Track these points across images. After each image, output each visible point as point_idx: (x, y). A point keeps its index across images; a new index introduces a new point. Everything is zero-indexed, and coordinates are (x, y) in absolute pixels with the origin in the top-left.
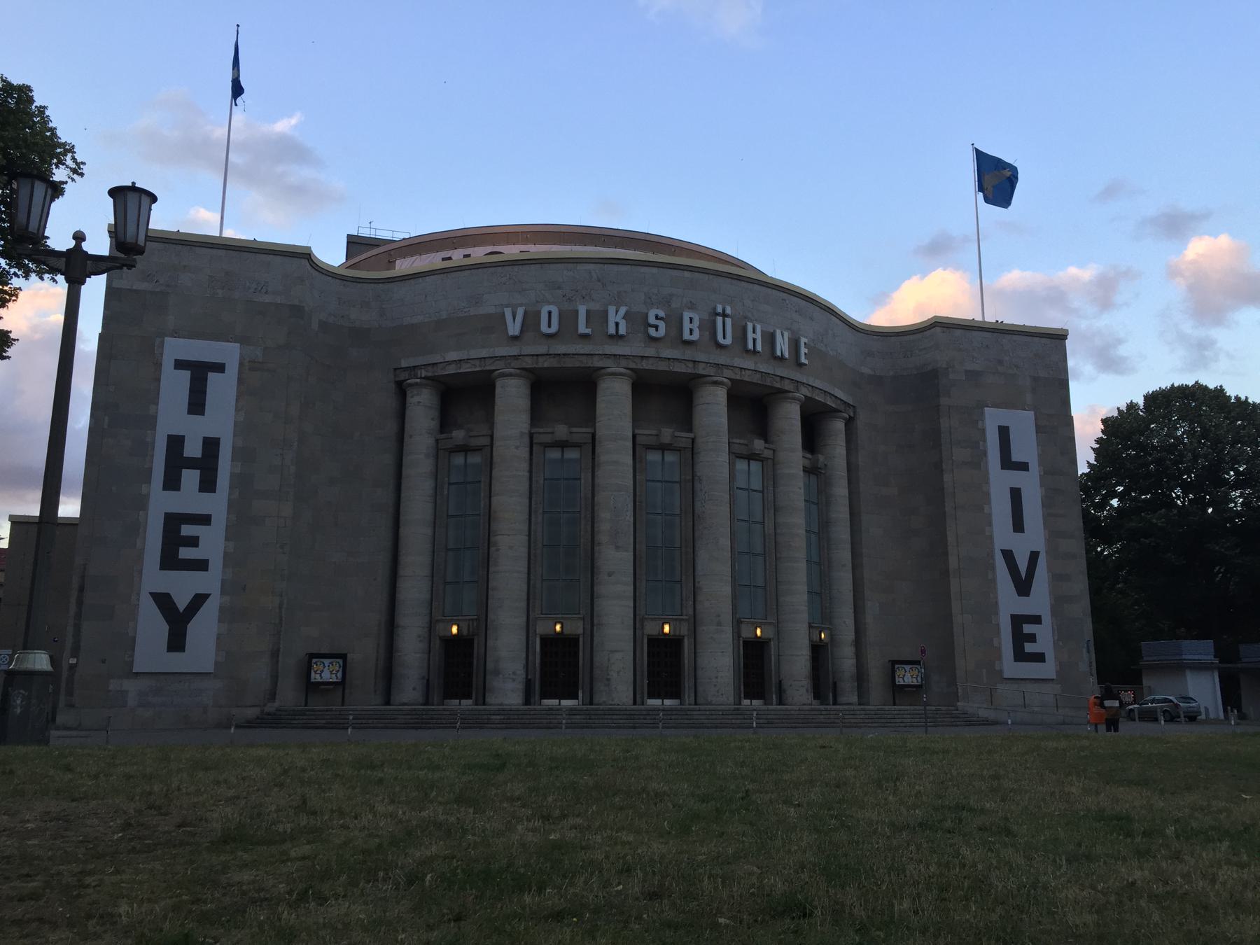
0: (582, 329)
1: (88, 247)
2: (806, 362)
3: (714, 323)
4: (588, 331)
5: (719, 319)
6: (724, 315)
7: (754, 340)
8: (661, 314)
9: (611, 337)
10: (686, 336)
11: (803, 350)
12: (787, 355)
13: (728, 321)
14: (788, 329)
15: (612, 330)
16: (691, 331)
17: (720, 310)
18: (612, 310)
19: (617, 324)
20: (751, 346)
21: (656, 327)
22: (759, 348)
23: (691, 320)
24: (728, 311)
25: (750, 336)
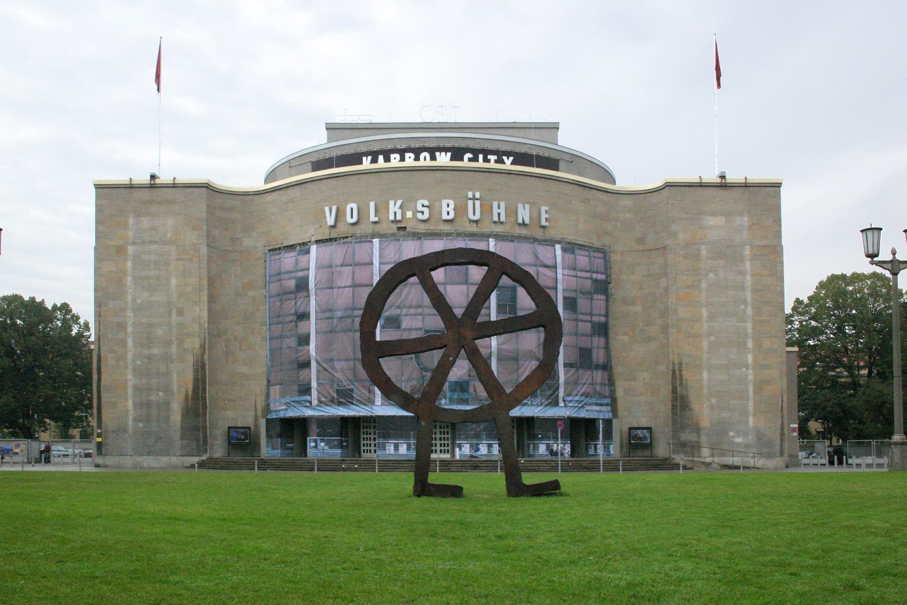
2: (546, 224)
4: (376, 219)
5: (470, 203)
6: (474, 199)
7: (499, 214)
8: (426, 203)
9: (393, 221)
13: (478, 203)
14: (529, 203)
15: (392, 217)
16: (448, 213)
17: (470, 195)
18: (391, 203)
21: (423, 212)
22: (503, 219)
23: (448, 206)
24: (478, 195)
25: (495, 211)
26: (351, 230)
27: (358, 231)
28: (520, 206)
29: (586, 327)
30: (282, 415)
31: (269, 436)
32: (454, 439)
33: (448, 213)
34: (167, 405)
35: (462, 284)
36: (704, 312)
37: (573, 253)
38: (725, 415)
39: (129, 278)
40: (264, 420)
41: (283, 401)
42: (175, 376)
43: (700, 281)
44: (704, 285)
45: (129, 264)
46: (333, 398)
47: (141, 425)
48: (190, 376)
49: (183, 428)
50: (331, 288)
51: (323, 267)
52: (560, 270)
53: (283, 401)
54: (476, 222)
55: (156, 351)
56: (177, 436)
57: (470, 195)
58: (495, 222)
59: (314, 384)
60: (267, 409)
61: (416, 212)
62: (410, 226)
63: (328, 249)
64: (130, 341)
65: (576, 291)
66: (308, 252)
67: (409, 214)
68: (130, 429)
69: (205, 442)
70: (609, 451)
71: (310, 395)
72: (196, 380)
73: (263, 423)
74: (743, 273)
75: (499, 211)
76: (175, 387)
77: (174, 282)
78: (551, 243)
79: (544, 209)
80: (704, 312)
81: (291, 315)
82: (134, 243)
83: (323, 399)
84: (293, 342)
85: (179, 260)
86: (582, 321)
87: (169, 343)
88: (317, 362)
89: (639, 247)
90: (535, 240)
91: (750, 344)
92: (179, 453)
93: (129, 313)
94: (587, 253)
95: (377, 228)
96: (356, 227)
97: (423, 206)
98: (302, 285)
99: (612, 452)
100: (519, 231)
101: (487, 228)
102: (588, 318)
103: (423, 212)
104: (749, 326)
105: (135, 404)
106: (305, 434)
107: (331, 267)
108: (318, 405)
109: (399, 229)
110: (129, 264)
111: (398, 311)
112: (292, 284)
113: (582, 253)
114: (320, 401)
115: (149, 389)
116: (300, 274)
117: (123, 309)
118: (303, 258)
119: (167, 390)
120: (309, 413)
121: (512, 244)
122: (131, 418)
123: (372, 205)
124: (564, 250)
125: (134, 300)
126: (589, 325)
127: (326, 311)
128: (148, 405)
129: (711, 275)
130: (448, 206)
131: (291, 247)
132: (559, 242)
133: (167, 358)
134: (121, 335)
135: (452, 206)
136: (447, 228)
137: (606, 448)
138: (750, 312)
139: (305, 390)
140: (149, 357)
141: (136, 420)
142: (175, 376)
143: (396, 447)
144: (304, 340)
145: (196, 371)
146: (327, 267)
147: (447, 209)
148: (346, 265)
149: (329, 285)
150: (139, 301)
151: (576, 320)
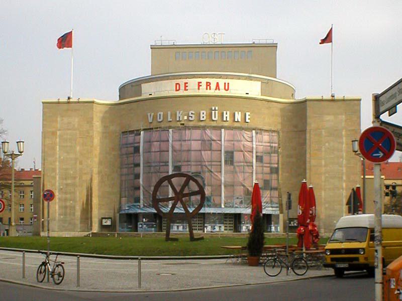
0: (169, 119)
1: (15, 153)
3: (212, 113)
4: (171, 120)
6: (215, 110)
7: (226, 117)
8: (193, 113)
9: (178, 121)
10: (202, 119)
11: (248, 117)
12: (240, 120)
15: (178, 119)
16: (203, 117)
17: (213, 109)
18: (178, 112)
19: (179, 117)
20: (225, 119)
21: (192, 117)
22: (228, 119)
23: (203, 114)
24: (217, 108)
26: (159, 125)
27: (163, 125)
28: (236, 113)
29: (267, 170)
30: (126, 212)
31: (120, 221)
32: (204, 223)
33: (203, 117)
34: (74, 207)
35: (209, 150)
36: (323, 163)
37: (261, 134)
38: (332, 212)
39: (58, 147)
40: (118, 214)
41: (127, 205)
42: (78, 193)
43: (321, 147)
44: (323, 149)
45: (58, 140)
46: (150, 204)
47: (62, 217)
48: (85, 192)
49: (81, 218)
50: (149, 152)
51: (147, 142)
52: (254, 143)
53: (127, 205)
54: (216, 121)
55: (69, 181)
56: (78, 222)
57: (213, 109)
58: (225, 121)
59: (142, 197)
60: (120, 209)
61: (188, 117)
62: (186, 124)
63: (148, 133)
64: (57, 177)
65: (262, 152)
66: (140, 134)
67: (186, 118)
68: (57, 218)
69: (91, 225)
70: (277, 230)
71: (140, 202)
72: (87, 196)
73: (118, 215)
74: (342, 143)
75: (226, 116)
76: (78, 199)
77: (78, 148)
78: (251, 130)
79: (248, 114)
80: (323, 163)
81: (132, 164)
82: (59, 130)
83: (146, 205)
84: (132, 177)
85: (80, 138)
86: (266, 167)
87: (75, 178)
88: (143, 187)
89: (296, 130)
90: (243, 129)
91: (344, 178)
92: (79, 230)
93: (57, 163)
94: (268, 134)
95: (172, 124)
96: (162, 123)
97: (192, 114)
98: (137, 150)
99: (279, 230)
100: (236, 125)
101: (221, 124)
102: (268, 165)
103: (192, 117)
104: (344, 170)
105: (60, 207)
106: (137, 221)
107: (150, 142)
108: (143, 207)
109: (181, 124)
110: (58, 140)
111: (180, 164)
112: (132, 150)
113: (266, 134)
114: (144, 206)
115: (66, 200)
116: (136, 145)
117: (55, 161)
118: (137, 137)
119: (74, 200)
120: (139, 211)
121: (232, 131)
122: (57, 214)
123: (169, 113)
124: (257, 133)
125: (60, 157)
126: (269, 168)
127: (148, 164)
128: (66, 207)
129: (327, 144)
130: (203, 114)
131: (131, 132)
132: (254, 130)
133: (74, 185)
134: (53, 174)
135: (205, 113)
136: (202, 124)
137: (276, 228)
138: (344, 162)
139: (137, 200)
140: (67, 185)
141: (60, 215)
142: (78, 193)
143: (178, 227)
144: (137, 176)
145: (88, 191)
146: (149, 142)
147: (204, 115)
148: (158, 141)
149: (148, 151)
150: (62, 158)
151: (263, 167)
